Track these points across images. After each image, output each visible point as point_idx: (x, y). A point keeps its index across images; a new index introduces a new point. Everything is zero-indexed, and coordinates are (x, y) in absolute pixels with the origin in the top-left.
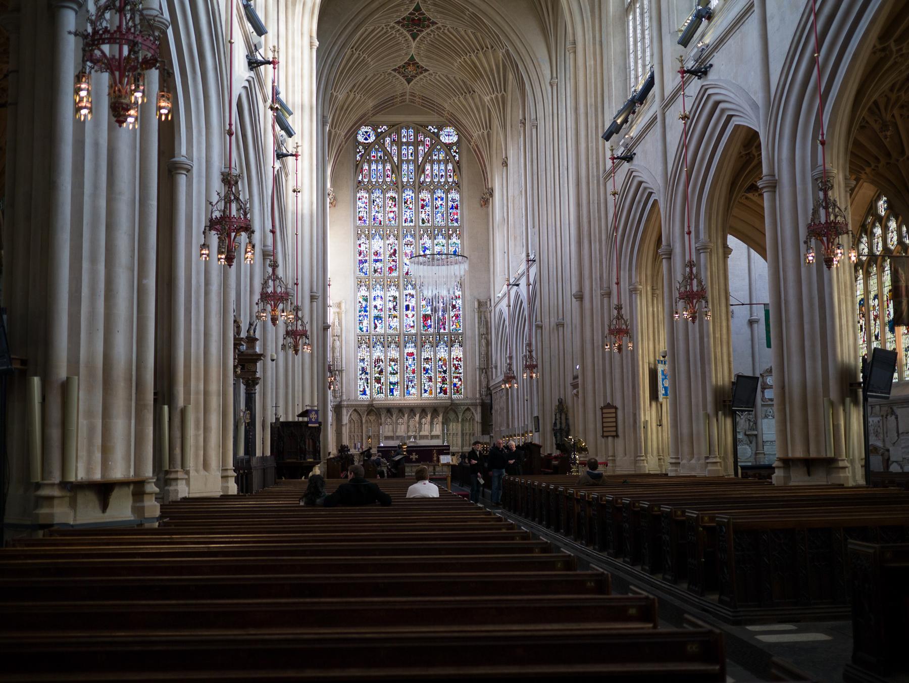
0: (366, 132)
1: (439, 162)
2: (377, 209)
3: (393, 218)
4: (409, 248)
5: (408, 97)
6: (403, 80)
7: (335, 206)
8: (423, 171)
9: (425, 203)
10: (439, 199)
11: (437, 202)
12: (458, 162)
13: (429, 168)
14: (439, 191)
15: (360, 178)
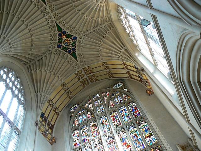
0: (75, 107)
1: (117, 97)
2: (85, 135)
3: (96, 134)
4: (112, 145)
5: (86, 76)
6: (70, 56)
7: (55, 142)
8: (109, 105)
9: (115, 117)
10: (123, 111)
11: (122, 113)
12: (128, 91)
13: (112, 102)
14: (122, 108)
15: (73, 126)
